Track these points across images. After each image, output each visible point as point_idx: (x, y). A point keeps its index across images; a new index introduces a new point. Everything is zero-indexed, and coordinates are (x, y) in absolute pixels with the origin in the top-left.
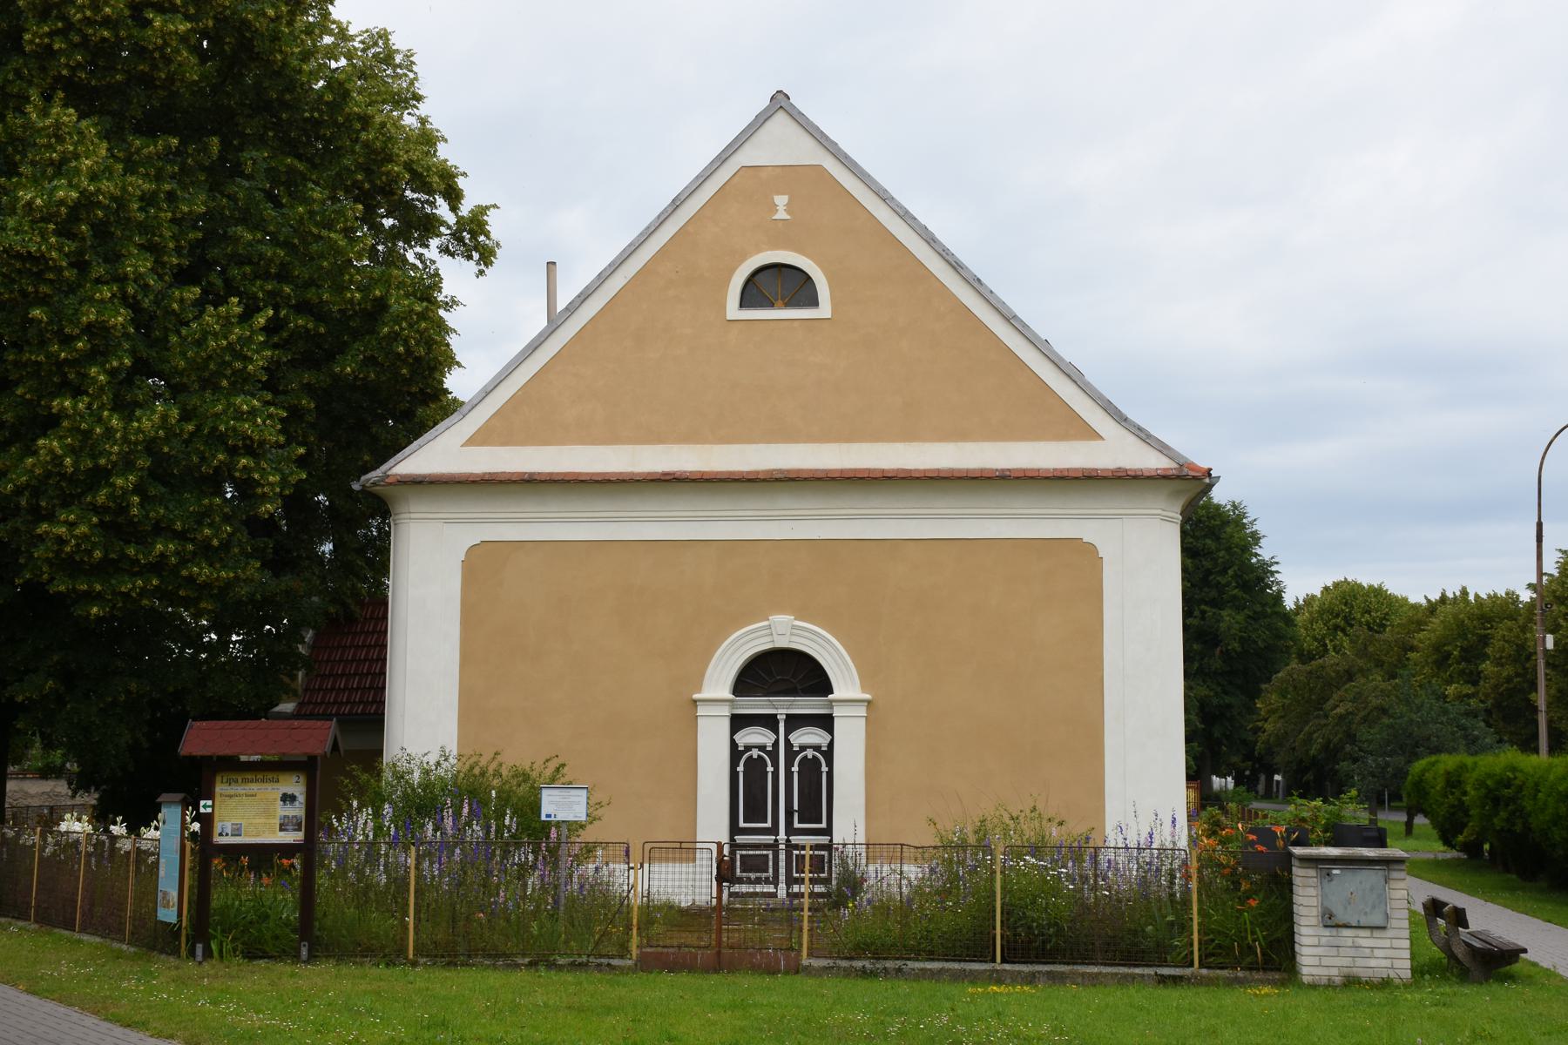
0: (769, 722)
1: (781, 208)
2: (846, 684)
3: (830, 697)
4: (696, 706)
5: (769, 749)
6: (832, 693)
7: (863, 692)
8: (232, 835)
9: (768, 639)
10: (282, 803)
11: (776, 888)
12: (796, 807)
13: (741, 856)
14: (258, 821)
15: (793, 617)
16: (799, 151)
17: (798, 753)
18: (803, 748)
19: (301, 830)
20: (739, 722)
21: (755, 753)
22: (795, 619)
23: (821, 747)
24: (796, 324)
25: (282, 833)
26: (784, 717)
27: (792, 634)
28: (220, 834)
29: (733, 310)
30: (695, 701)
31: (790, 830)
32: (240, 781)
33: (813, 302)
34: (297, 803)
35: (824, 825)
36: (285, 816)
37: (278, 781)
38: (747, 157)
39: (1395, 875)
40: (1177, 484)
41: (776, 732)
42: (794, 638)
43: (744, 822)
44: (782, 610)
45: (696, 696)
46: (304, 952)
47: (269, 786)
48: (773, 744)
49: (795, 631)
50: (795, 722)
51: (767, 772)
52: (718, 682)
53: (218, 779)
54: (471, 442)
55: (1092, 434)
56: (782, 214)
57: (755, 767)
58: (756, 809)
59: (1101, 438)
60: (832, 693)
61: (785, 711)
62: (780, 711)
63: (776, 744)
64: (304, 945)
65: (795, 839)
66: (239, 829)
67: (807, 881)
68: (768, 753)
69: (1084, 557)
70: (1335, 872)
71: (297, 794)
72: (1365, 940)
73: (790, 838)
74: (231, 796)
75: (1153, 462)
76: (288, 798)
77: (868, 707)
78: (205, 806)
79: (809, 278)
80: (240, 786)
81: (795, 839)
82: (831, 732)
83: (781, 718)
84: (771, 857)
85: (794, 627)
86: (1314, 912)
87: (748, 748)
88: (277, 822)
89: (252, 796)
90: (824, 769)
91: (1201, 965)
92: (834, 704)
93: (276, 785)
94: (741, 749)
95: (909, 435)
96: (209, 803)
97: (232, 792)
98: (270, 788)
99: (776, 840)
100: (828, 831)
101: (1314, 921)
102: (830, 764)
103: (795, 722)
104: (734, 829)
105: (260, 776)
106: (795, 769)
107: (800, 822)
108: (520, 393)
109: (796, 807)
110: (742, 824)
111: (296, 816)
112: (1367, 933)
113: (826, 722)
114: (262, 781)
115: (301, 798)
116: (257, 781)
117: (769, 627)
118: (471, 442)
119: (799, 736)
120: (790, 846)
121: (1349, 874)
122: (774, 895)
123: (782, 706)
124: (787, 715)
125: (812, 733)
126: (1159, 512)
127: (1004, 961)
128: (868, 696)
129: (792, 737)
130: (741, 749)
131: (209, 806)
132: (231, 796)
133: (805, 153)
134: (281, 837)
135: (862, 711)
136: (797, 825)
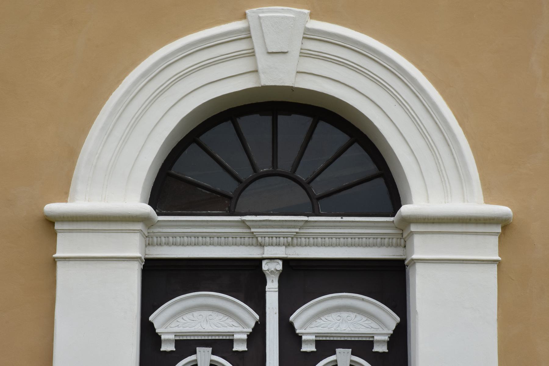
4: (54, 234)
5: (240, 347)
7: (488, 200)
9: (243, 65)
15: (307, 11)
22: (312, 16)
23: (371, 343)
26: (279, 266)
27: (304, 54)
48: (251, 337)
62: (269, 252)
77: (502, 237)
92: (413, 228)
94: (167, 347)
119: (319, 315)
124: (286, 262)
130: (167, 347)
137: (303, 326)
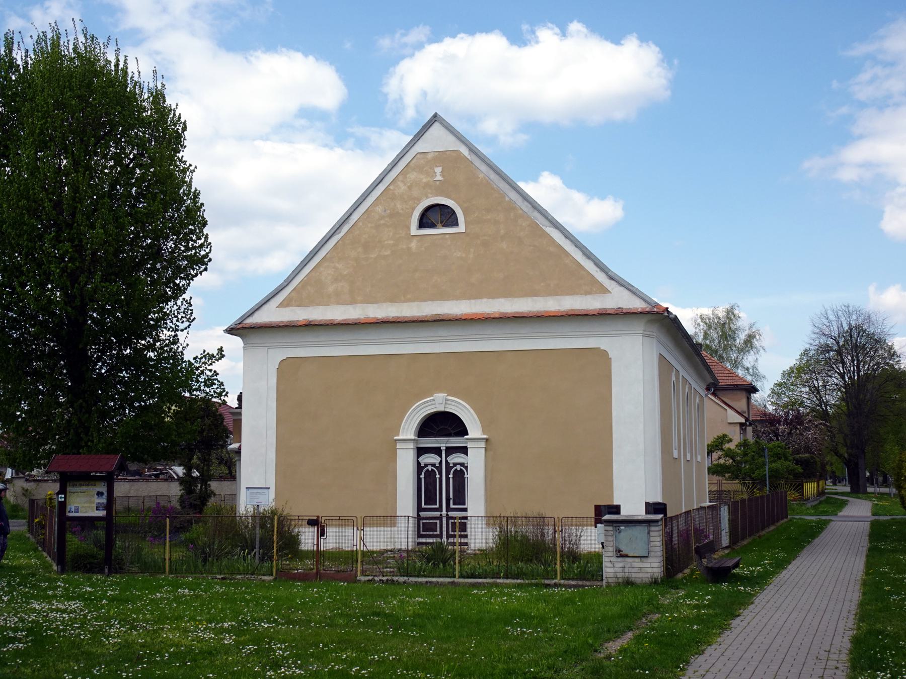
0: (437, 451)
1: (438, 174)
2: (474, 430)
3: (466, 437)
5: (437, 465)
6: (467, 434)
7: (484, 434)
12: (451, 496)
13: (423, 523)
14: (86, 505)
16: (449, 143)
17: (452, 467)
20: (421, 451)
21: (430, 468)
22: (448, 395)
24: (447, 236)
25: (97, 511)
26: (444, 448)
28: (69, 512)
29: (414, 229)
30: (396, 440)
31: (448, 509)
33: (455, 223)
36: (99, 503)
37: (95, 485)
38: (419, 147)
39: (653, 528)
40: (649, 317)
41: (441, 456)
42: (447, 406)
44: (440, 390)
45: (396, 438)
46: (106, 571)
47: (91, 488)
50: (450, 451)
52: (408, 430)
53: (68, 484)
54: (281, 305)
55: (605, 290)
56: (439, 178)
57: (430, 475)
58: (430, 499)
60: (467, 434)
61: (444, 445)
62: (442, 445)
63: (441, 463)
65: (451, 514)
66: (78, 509)
67: (457, 536)
68: (437, 468)
69: (601, 358)
70: (622, 528)
71: (104, 492)
72: (637, 563)
74: (74, 493)
75: (639, 305)
76: (100, 494)
77: (486, 442)
78: (61, 498)
79: (454, 212)
81: (451, 514)
83: (443, 448)
84: (424, 521)
85: (446, 400)
86: (611, 549)
87: (426, 465)
88: (95, 506)
91: (562, 578)
93: (94, 488)
94: (423, 465)
95: (507, 294)
96: (63, 496)
97: (75, 491)
99: (441, 515)
101: (610, 554)
103: (450, 451)
104: (420, 509)
106: (451, 476)
109: (451, 496)
110: (423, 506)
112: (638, 560)
113: (464, 450)
114: (88, 485)
115: (105, 494)
116: (85, 485)
117: (433, 400)
118: (281, 305)
120: (448, 518)
121: (627, 528)
123: (443, 443)
125: (456, 457)
126: (641, 332)
127: (459, 577)
128: (485, 436)
129: (449, 459)
130: (423, 465)
133: (450, 144)
135: (483, 444)
136: (452, 506)
137: (450, 460)
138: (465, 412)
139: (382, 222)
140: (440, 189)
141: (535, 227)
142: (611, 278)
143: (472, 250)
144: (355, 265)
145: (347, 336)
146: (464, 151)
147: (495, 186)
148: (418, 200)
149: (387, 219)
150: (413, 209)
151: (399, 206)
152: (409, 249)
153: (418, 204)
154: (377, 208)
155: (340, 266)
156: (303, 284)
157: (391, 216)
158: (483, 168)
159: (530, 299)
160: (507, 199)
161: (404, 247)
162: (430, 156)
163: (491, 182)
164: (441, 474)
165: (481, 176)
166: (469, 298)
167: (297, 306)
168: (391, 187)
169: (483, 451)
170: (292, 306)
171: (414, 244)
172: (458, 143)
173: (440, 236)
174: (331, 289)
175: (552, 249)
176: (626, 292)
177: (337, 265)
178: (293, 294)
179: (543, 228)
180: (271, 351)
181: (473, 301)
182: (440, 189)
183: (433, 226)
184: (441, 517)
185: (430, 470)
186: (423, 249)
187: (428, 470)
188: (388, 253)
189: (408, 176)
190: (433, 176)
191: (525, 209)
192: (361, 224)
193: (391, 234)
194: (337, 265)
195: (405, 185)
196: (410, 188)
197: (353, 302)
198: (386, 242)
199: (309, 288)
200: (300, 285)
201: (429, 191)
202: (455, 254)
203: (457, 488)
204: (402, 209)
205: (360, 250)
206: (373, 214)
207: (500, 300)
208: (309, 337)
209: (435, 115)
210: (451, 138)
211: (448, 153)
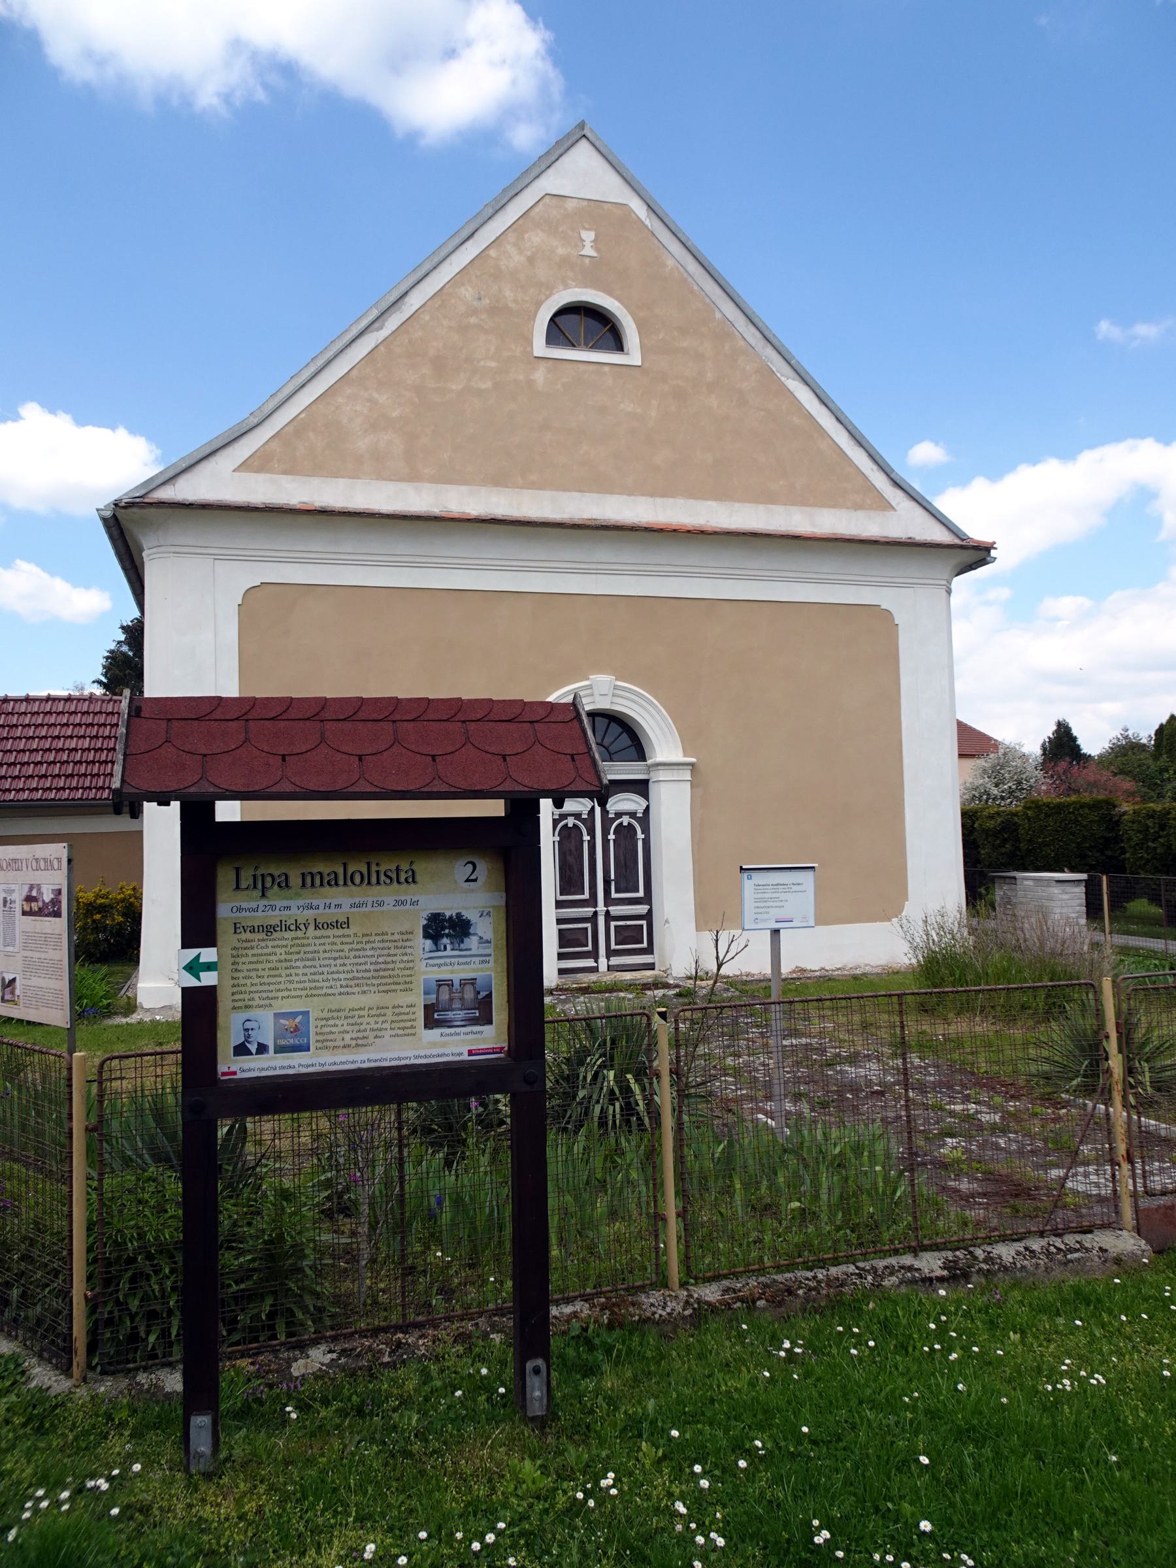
1: (588, 244)
7: (685, 755)
8: (280, 1050)
10: (429, 943)
11: (596, 961)
12: (613, 877)
17: (614, 820)
18: (619, 815)
19: (490, 1022)
24: (607, 369)
28: (241, 1050)
31: (608, 901)
32: (295, 880)
34: (472, 942)
35: (641, 894)
36: (440, 983)
38: (550, 183)
43: (583, 894)
47: (388, 894)
49: (617, 692)
51: (582, 841)
54: (244, 466)
55: (885, 505)
56: (589, 251)
59: (893, 508)
64: (537, 1371)
65: (615, 910)
68: (583, 821)
71: (470, 915)
73: (610, 908)
74: (269, 930)
75: (940, 535)
80: (298, 895)
81: (615, 910)
82: (646, 797)
85: (616, 687)
88: (418, 1000)
89: (337, 925)
90: (640, 836)
93: (407, 892)
95: (721, 493)
97: (273, 918)
98: (390, 900)
99: (596, 913)
100: (648, 899)
102: (646, 830)
105: (357, 866)
106: (612, 837)
107: (617, 891)
108: (303, 416)
109: (613, 877)
111: (473, 981)
114: (366, 880)
116: (349, 880)
118: (244, 466)
122: (595, 970)
128: (693, 760)
131: (209, 967)
132: (269, 930)
134: (434, 1045)
136: (614, 895)
138: (649, 713)
139: (473, 320)
140: (591, 275)
141: (768, 373)
142: (897, 484)
143: (654, 403)
144: (416, 400)
145: (404, 545)
146: (638, 208)
147: (696, 287)
148: (549, 289)
149: (483, 317)
150: (538, 304)
151: (508, 293)
152: (530, 383)
153: (548, 297)
154: (463, 290)
155: (382, 398)
156: (298, 427)
157: (493, 311)
158: (675, 247)
159: (761, 507)
160: (718, 315)
161: (521, 377)
162: (570, 205)
163: (690, 279)
164: (592, 832)
165: (670, 262)
166: (652, 495)
167: (285, 473)
168: (492, 253)
169: (688, 785)
170: (269, 471)
171: (540, 375)
172: (627, 191)
173: (591, 367)
174: (363, 444)
175: (796, 420)
176: (919, 511)
177: (376, 395)
178: (273, 445)
179: (783, 379)
180: (222, 568)
181: (659, 500)
182: (591, 275)
183: (571, 344)
184: (594, 918)
185: (570, 825)
186: (559, 387)
187: (566, 825)
188: (487, 385)
189: (526, 236)
190: (576, 246)
191: (752, 341)
192: (427, 318)
193: (493, 349)
194: (376, 395)
195: (521, 251)
196: (531, 260)
197: (413, 477)
198: (482, 363)
199: (312, 435)
200: (290, 429)
201: (570, 274)
202: (622, 406)
203: (622, 858)
204: (515, 301)
205: (426, 370)
206: (453, 301)
207: (709, 503)
208: (318, 543)
209: (582, 125)
210: (613, 179)
211: (606, 206)
